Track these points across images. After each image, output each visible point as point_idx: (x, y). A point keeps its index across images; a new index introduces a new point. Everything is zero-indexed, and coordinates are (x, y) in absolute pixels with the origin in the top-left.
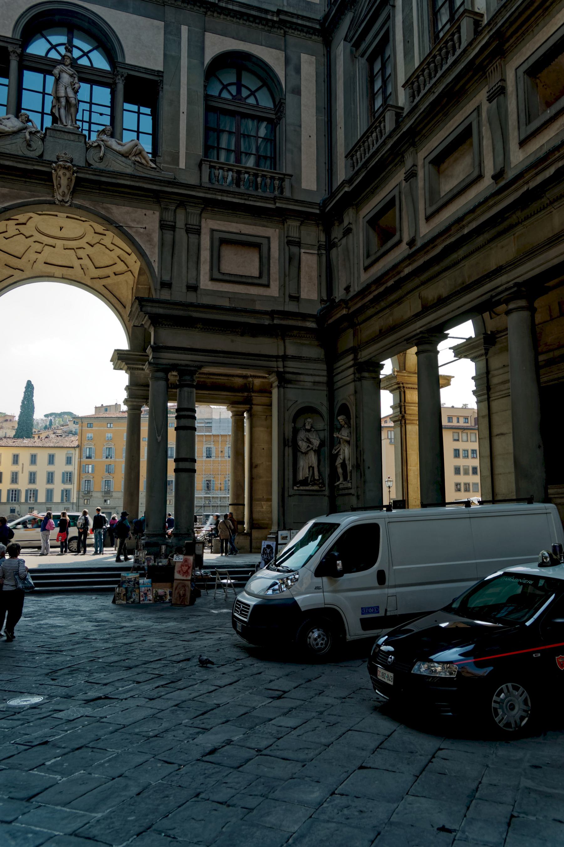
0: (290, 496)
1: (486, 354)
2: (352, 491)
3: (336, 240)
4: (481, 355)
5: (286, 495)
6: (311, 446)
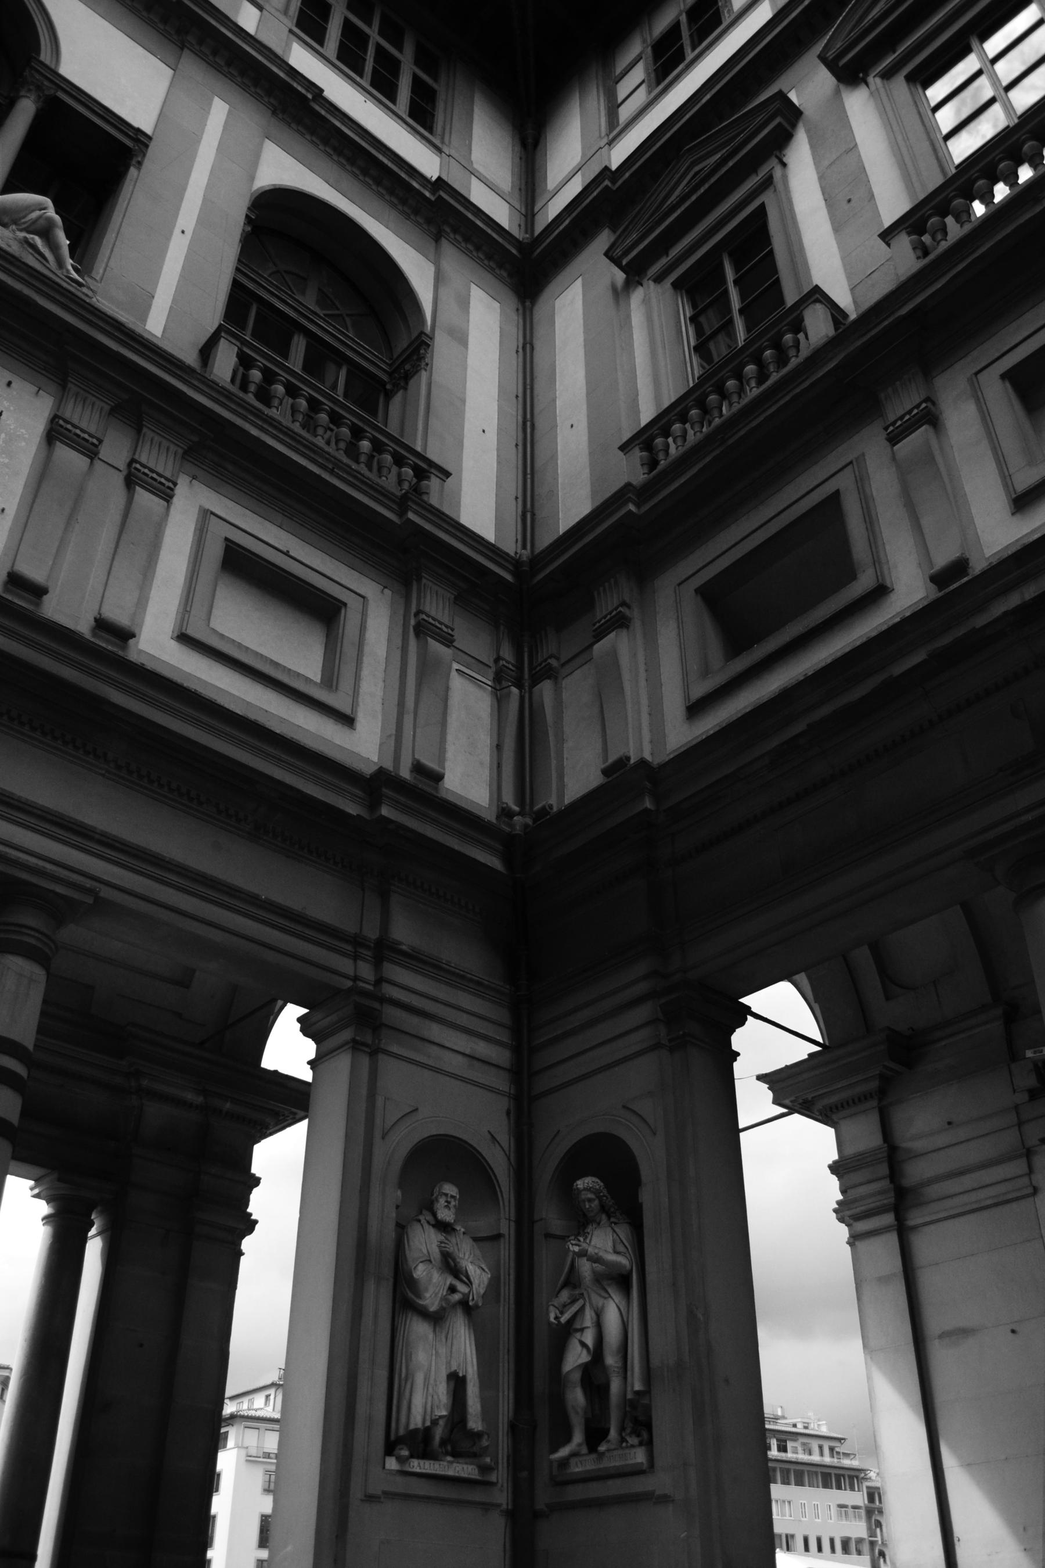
0: (370, 1498)
1: (882, 1093)
2: (659, 1482)
3: (554, 662)
4: (864, 1097)
5: (356, 1492)
6: (462, 1288)
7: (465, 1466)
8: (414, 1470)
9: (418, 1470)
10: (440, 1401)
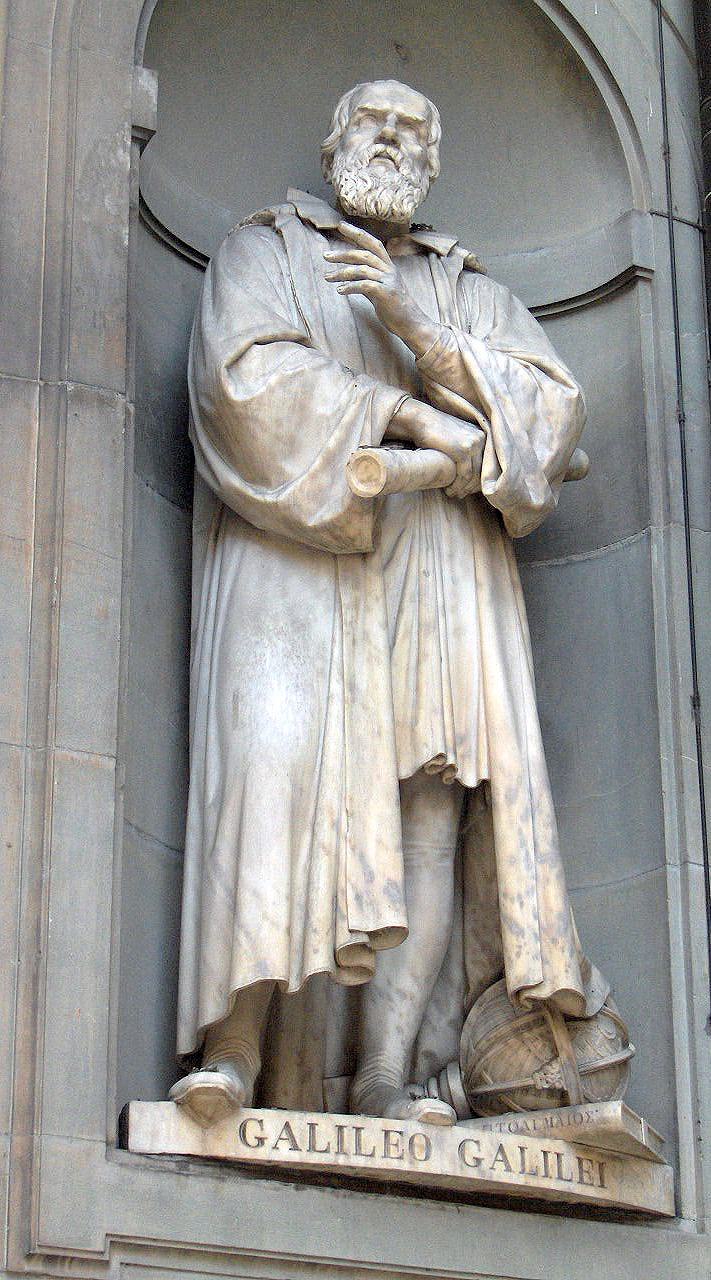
7: (512, 1142)
8: (263, 1154)
9: (284, 1155)
10: (370, 877)
